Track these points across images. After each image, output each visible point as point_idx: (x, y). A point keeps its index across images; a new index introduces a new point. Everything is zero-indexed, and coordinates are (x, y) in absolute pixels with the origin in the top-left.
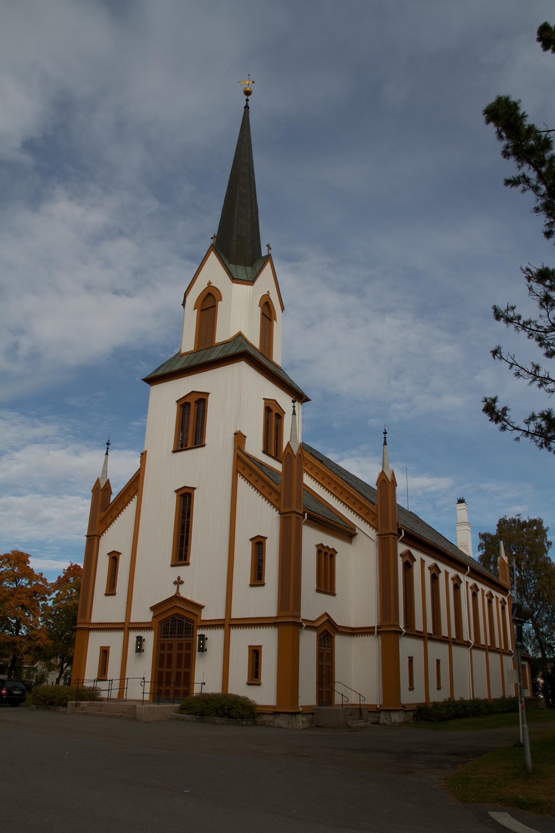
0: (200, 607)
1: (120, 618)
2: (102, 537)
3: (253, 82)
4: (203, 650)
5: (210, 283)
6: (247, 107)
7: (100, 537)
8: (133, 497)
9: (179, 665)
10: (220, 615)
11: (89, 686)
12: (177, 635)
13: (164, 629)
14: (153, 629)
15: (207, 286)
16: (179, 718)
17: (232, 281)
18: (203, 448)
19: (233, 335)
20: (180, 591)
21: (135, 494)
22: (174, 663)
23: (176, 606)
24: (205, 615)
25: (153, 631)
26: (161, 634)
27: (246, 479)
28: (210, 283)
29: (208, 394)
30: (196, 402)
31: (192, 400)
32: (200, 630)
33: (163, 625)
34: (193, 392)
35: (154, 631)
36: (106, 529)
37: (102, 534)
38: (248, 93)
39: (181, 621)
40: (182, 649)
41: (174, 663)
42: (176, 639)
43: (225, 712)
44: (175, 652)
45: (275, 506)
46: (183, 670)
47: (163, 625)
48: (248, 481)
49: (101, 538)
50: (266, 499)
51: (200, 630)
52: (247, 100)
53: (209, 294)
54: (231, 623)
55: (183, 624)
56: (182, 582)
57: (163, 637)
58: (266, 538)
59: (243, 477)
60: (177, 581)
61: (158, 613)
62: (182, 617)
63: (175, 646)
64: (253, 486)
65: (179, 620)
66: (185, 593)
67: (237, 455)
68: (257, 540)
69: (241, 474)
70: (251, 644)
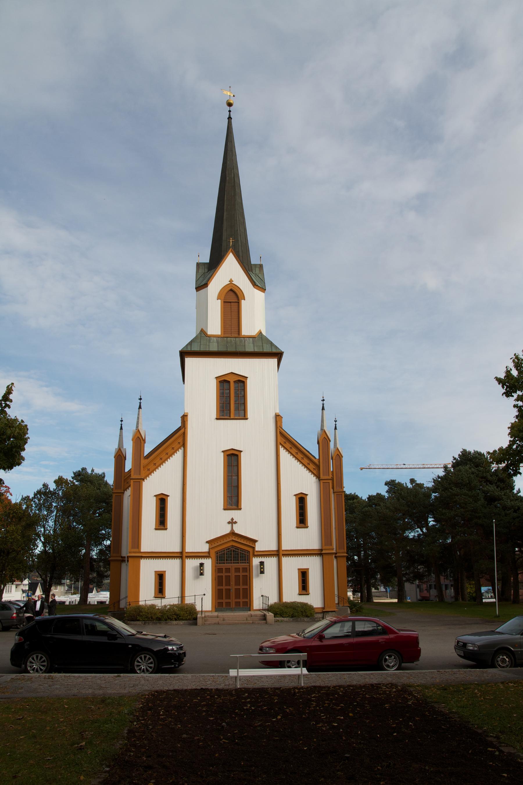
0: (255, 541)
1: (177, 549)
2: (145, 480)
3: (234, 96)
4: (262, 572)
5: (231, 281)
6: (230, 118)
7: (143, 480)
8: (178, 450)
9: (237, 583)
10: (274, 547)
11: (150, 604)
12: (233, 562)
13: (220, 557)
14: (211, 557)
15: (229, 283)
16: (278, 621)
17: (254, 287)
18: (246, 420)
19: (257, 332)
20: (234, 529)
21: (180, 448)
22: (233, 582)
23: (233, 540)
24: (259, 547)
25: (210, 559)
26: (218, 561)
27: (287, 450)
28: (231, 281)
29: (247, 378)
30: (234, 382)
31: (232, 380)
32: (255, 558)
33: (219, 554)
34: (232, 373)
35: (211, 559)
36: (150, 474)
37: (146, 477)
38: (230, 105)
39: (236, 551)
40: (226, 572)
41: (233, 582)
42: (233, 565)
43: (307, 614)
44: (233, 574)
45: (313, 473)
46: (241, 587)
47: (219, 554)
48: (290, 452)
49: (144, 481)
50: (306, 467)
51: (255, 558)
52: (230, 111)
53: (231, 290)
54: (283, 553)
55: (238, 554)
56: (236, 522)
57: (220, 563)
58: (307, 495)
59: (285, 448)
60: (231, 521)
61: (214, 545)
62: (237, 548)
63: (233, 570)
64: (294, 456)
65: (234, 551)
66: (238, 530)
67: (280, 432)
68: (300, 496)
69: (283, 446)
70: (299, 568)
